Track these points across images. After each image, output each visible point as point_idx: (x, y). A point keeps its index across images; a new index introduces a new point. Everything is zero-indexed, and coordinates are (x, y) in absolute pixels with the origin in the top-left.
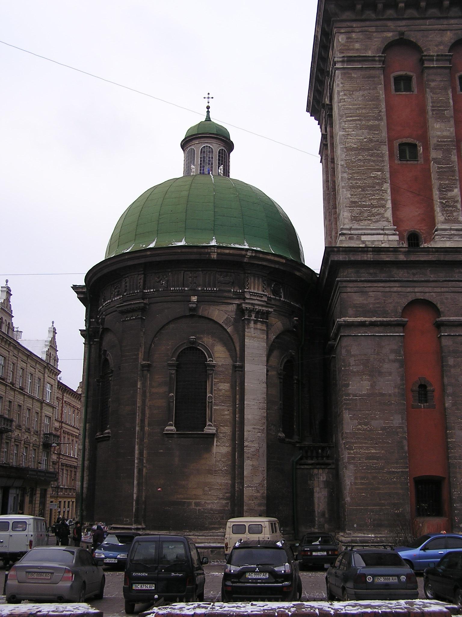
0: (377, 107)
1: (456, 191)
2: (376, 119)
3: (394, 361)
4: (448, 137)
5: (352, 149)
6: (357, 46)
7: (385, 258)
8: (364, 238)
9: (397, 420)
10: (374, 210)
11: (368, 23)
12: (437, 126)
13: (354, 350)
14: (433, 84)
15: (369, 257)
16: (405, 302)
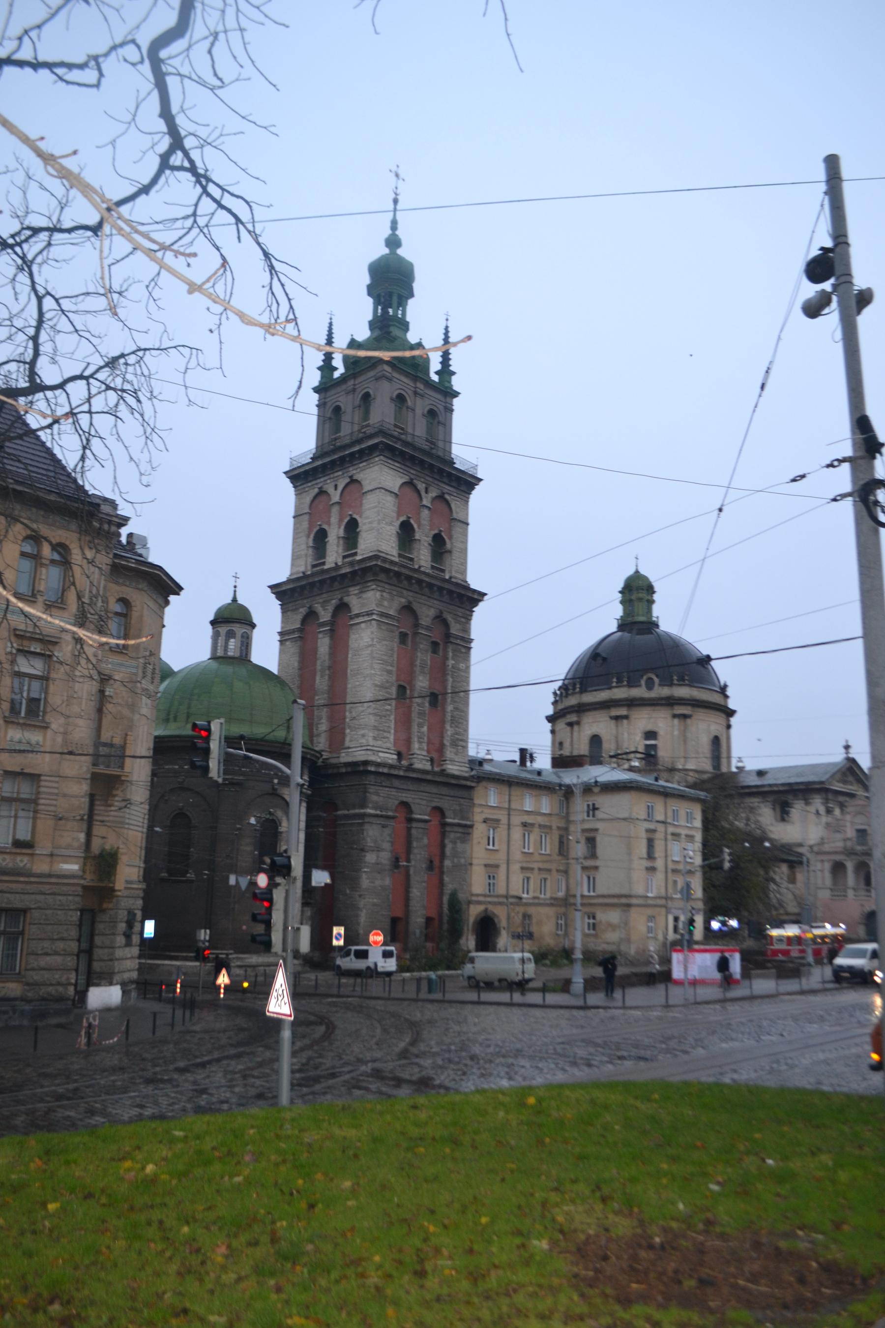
0: (392, 656)
1: (425, 729)
2: (392, 666)
3: (389, 842)
4: (424, 688)
5: (377, 686)
6: (386, 603)
7: (396, 772)
8: (381, 754)
9: (388, 881)
10: (385, 734)
11: (393, 588)
12: (421, 678)
13: (371, 833)
14: (422, 646)
15: (385, 770)
16: (397, 802)
